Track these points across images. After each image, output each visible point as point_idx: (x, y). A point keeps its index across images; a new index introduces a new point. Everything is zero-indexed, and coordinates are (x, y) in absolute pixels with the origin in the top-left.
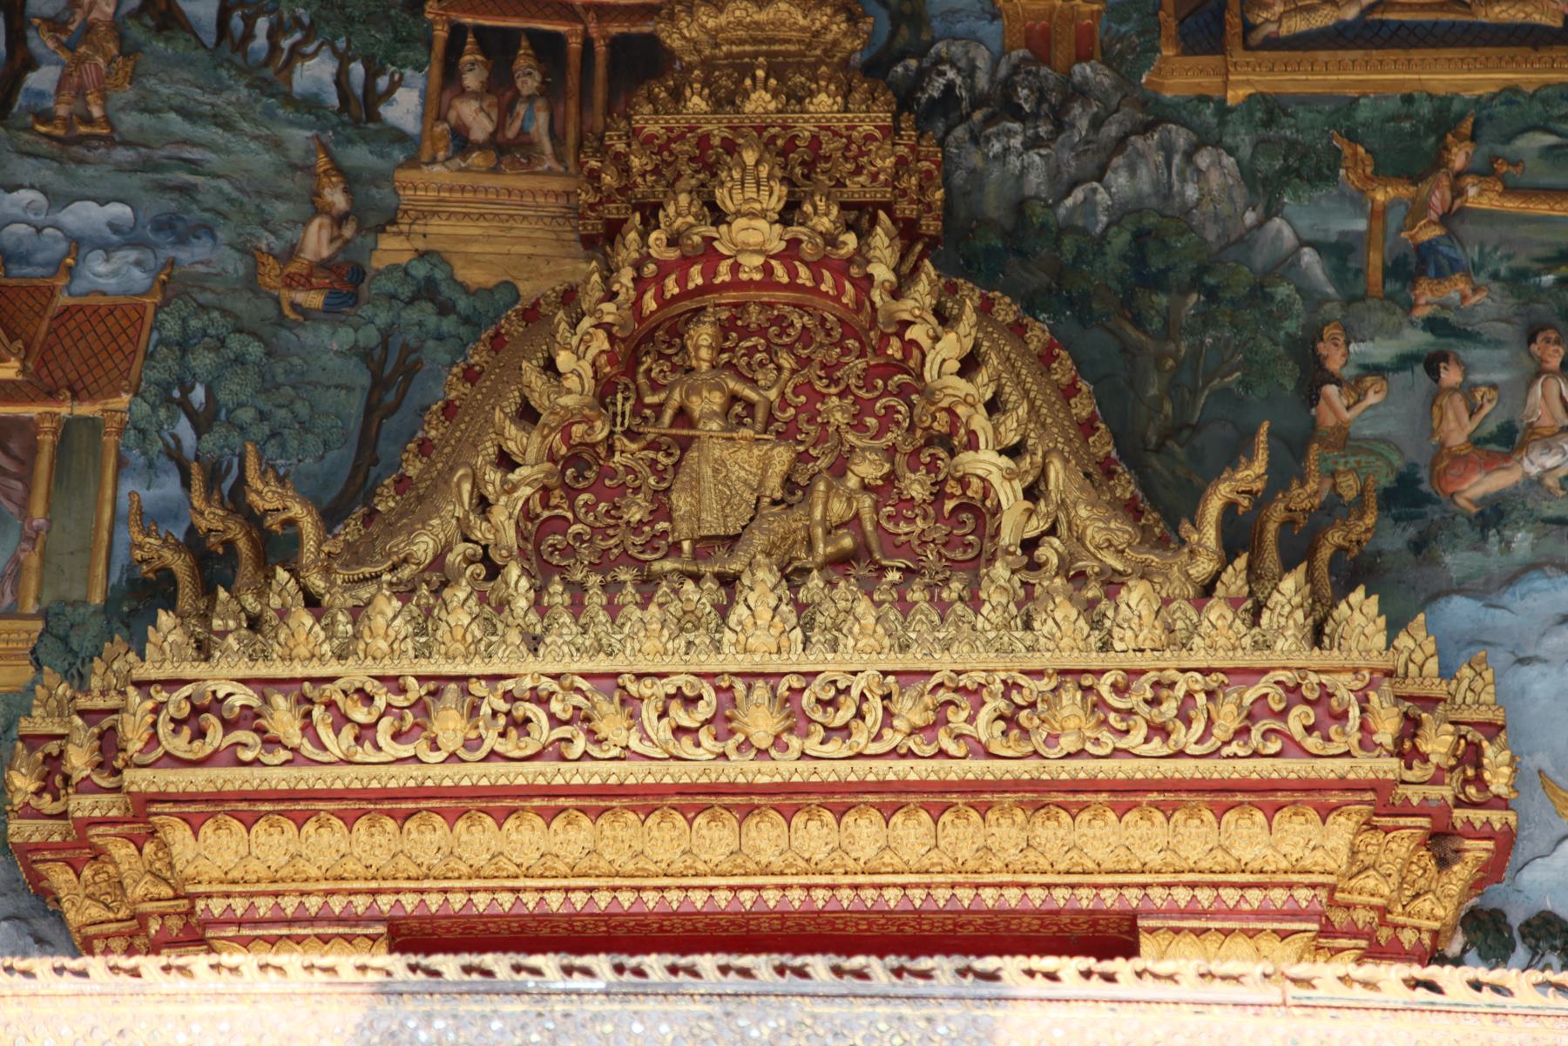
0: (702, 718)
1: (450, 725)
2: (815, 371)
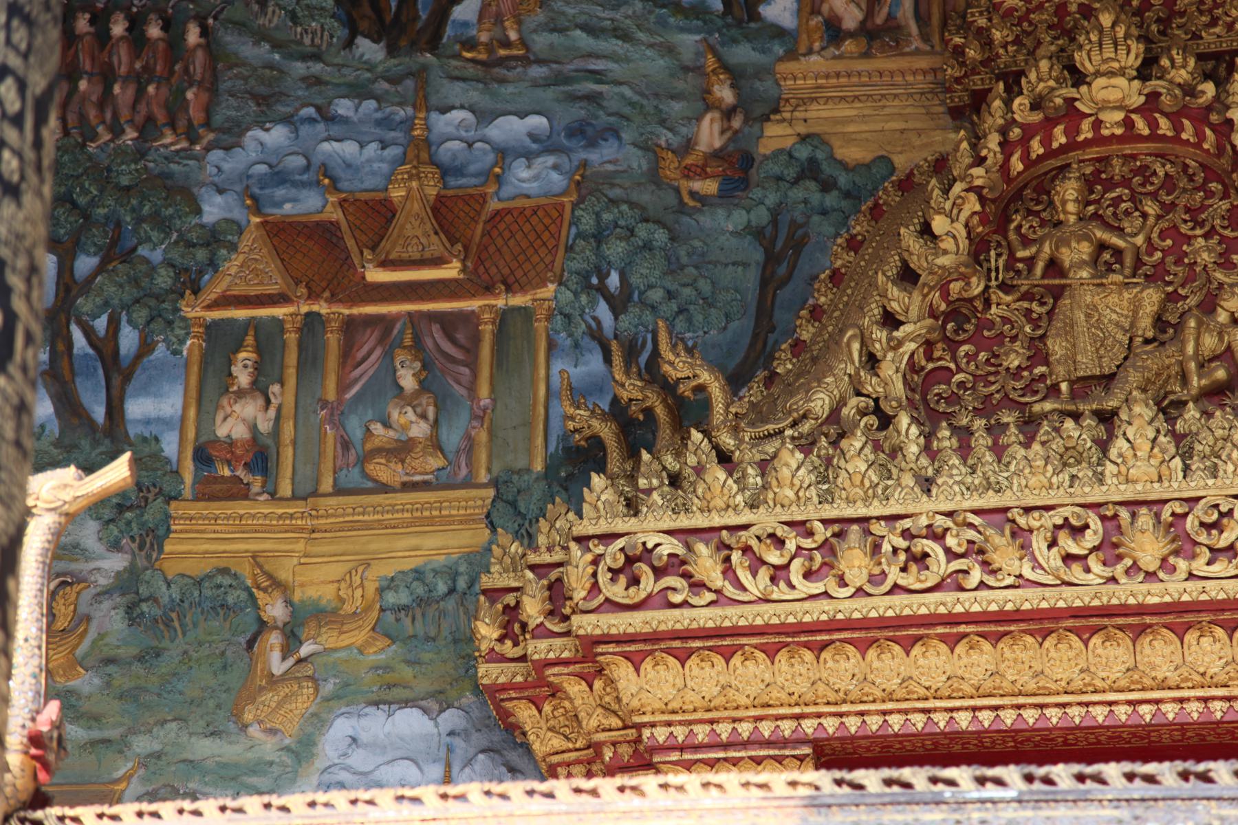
0: (1090, 545)
1: (855, 563)
2: (1179, 215)
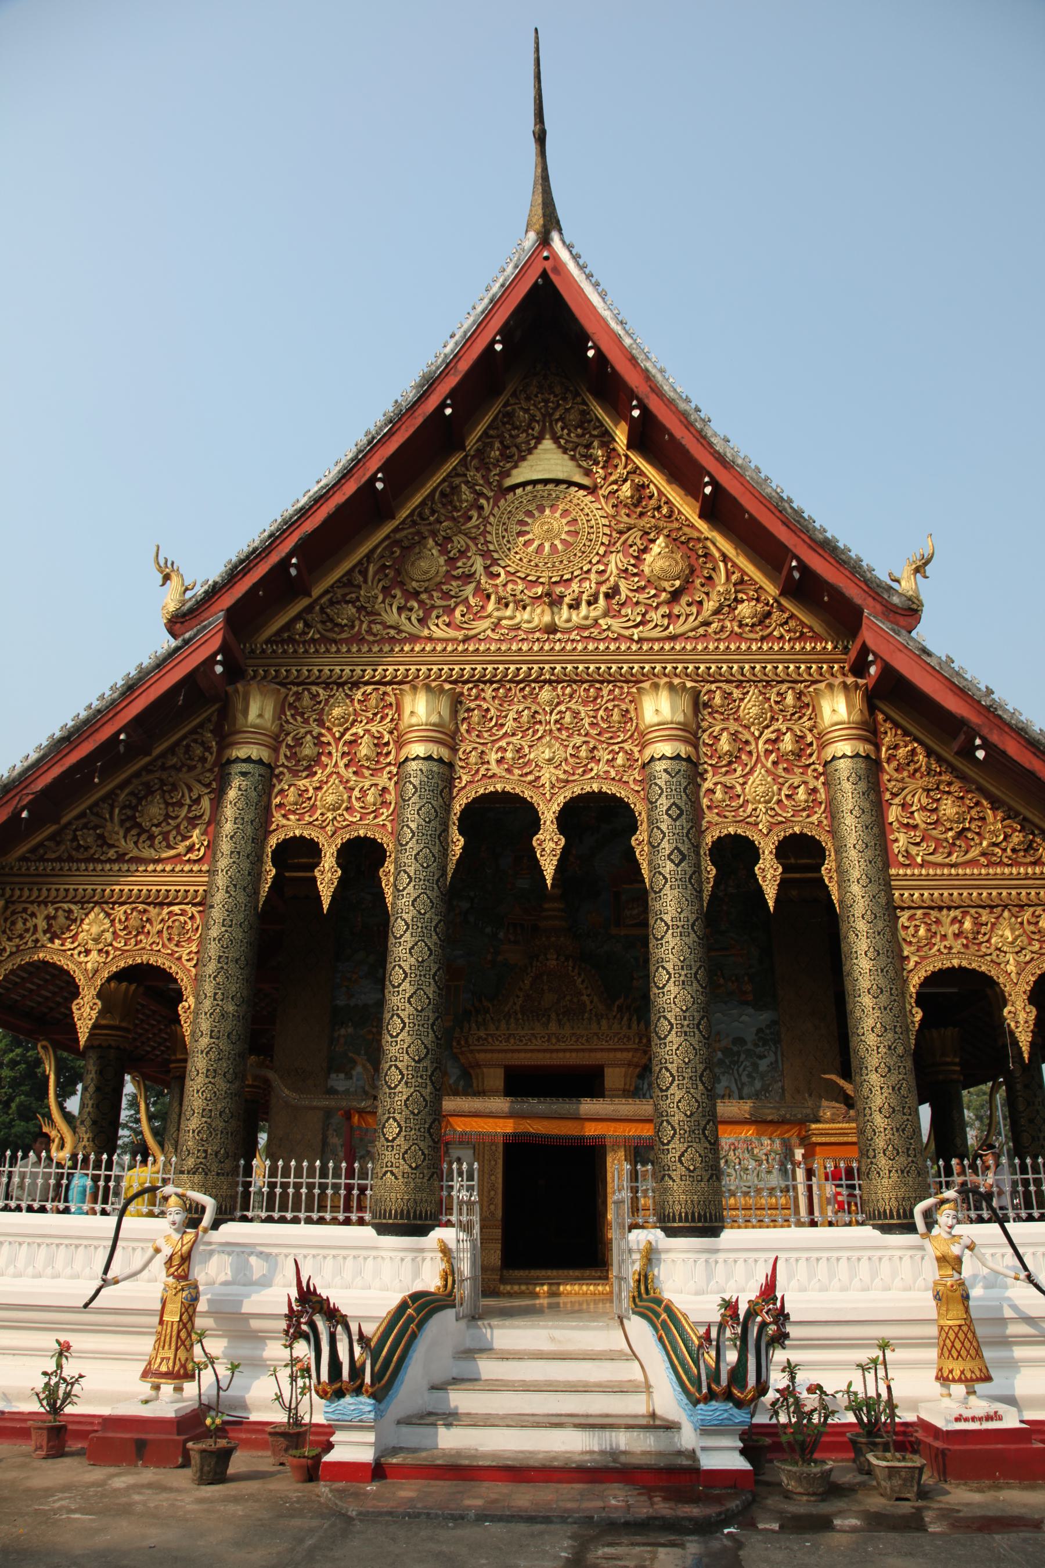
1: (512, 1041)
